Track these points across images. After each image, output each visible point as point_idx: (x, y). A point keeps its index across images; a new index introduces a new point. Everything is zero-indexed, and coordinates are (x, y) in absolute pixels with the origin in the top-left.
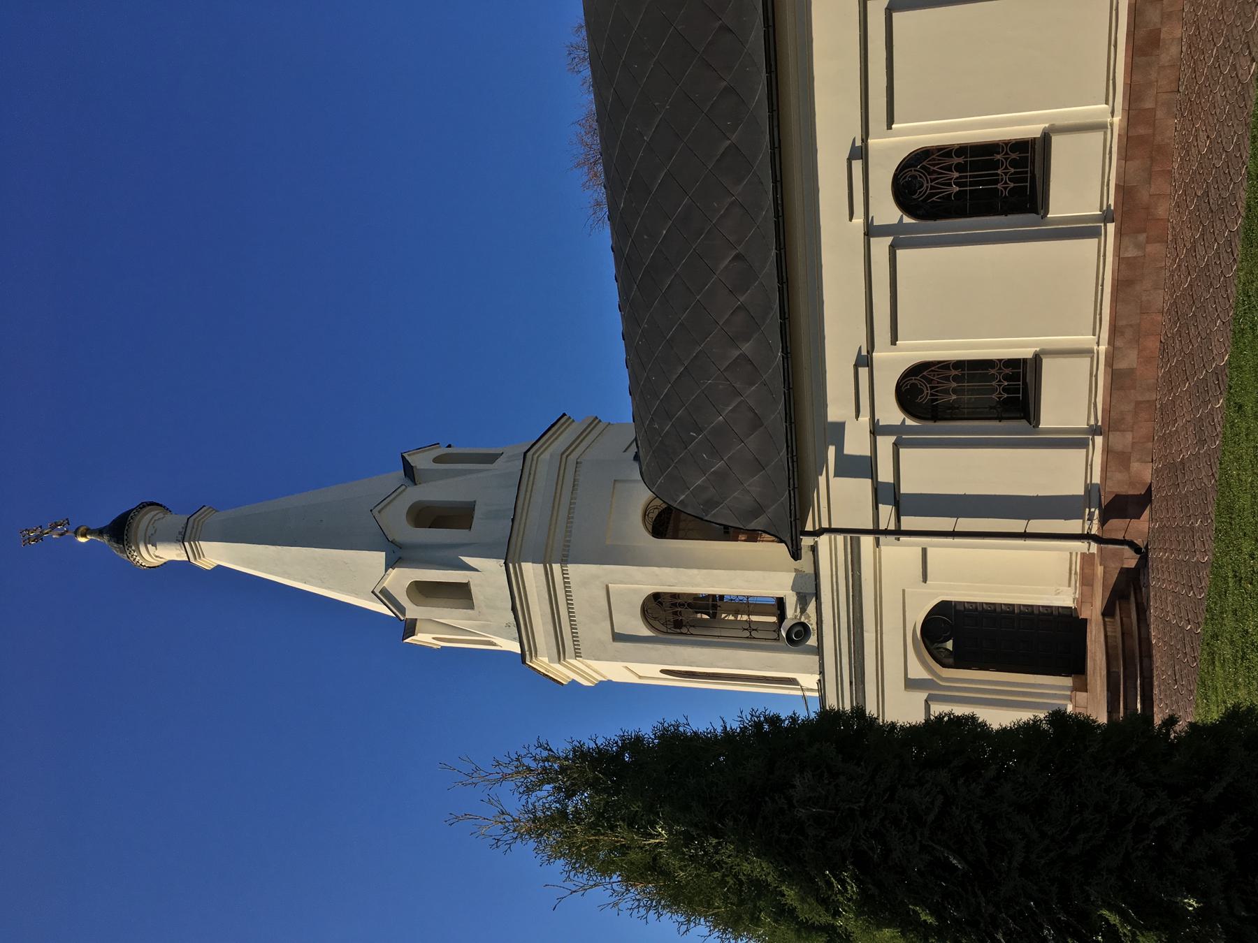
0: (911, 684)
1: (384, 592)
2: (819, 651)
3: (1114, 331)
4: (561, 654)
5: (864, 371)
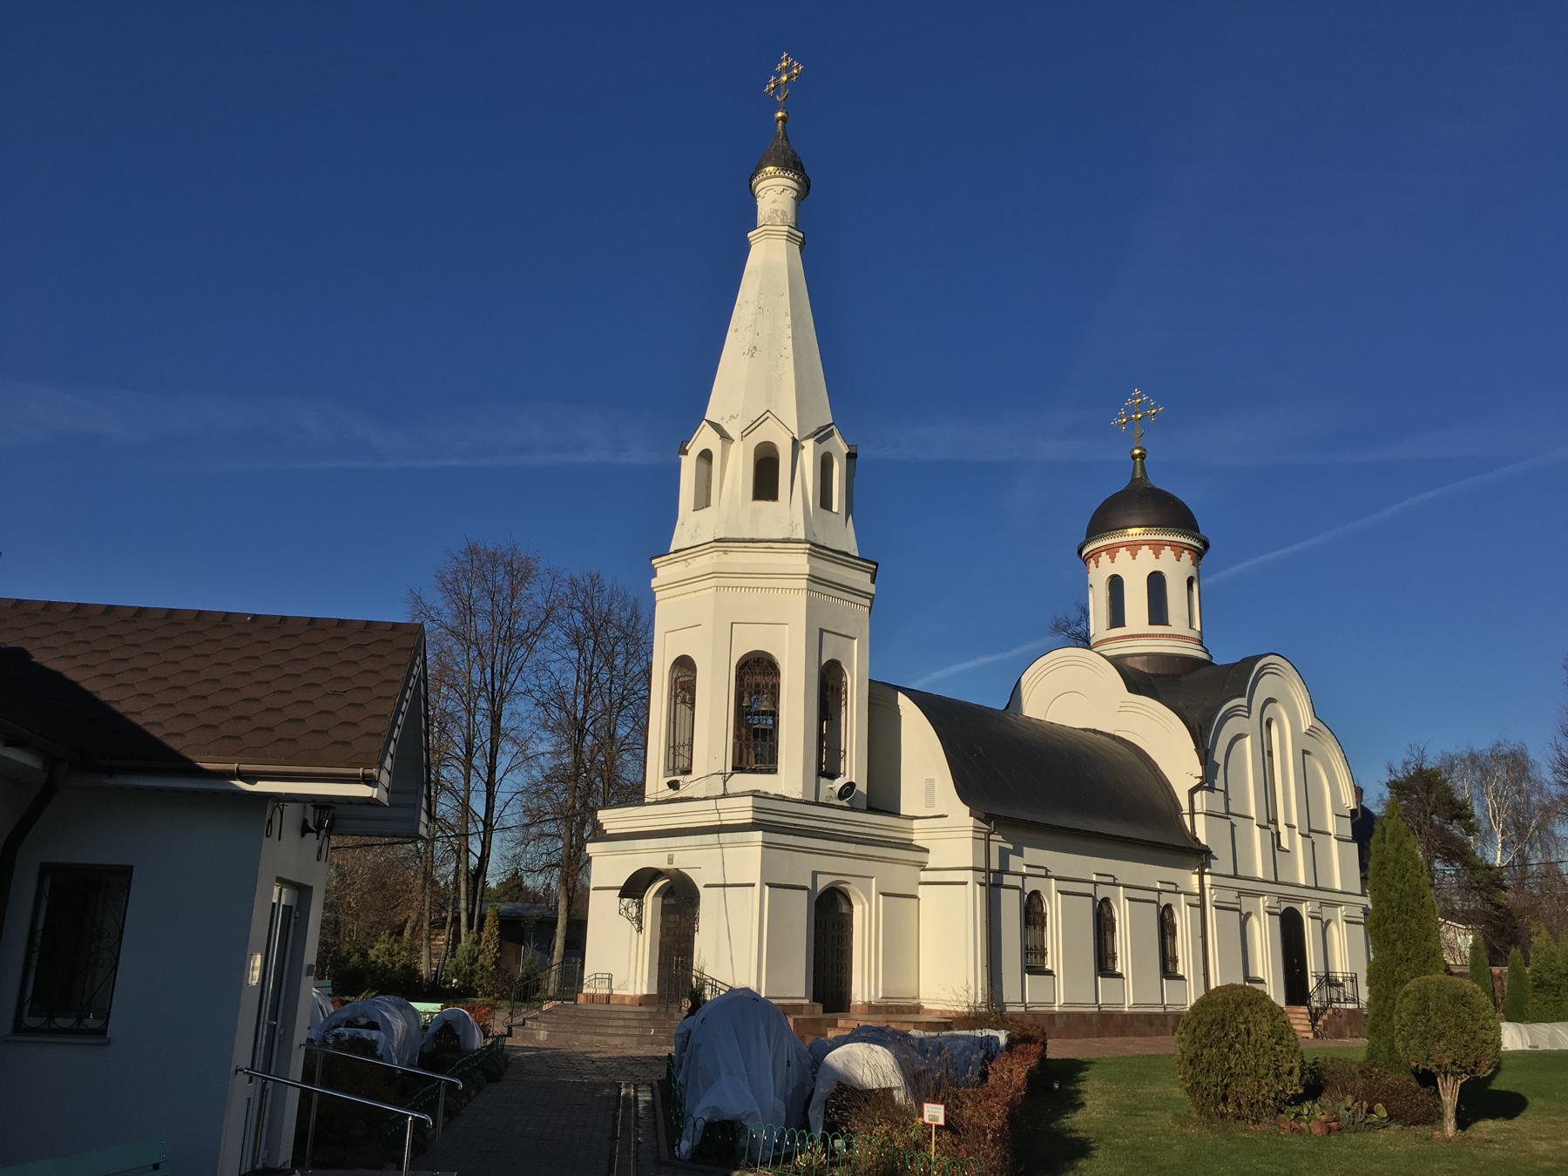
0: (815, 874)
1: (831, 434)
2: (817, 803)
3: (1068, 1014)
4: (814, 579)
5: (1042, 872)
